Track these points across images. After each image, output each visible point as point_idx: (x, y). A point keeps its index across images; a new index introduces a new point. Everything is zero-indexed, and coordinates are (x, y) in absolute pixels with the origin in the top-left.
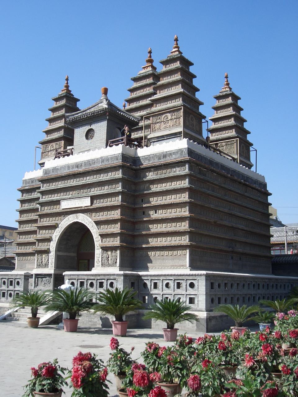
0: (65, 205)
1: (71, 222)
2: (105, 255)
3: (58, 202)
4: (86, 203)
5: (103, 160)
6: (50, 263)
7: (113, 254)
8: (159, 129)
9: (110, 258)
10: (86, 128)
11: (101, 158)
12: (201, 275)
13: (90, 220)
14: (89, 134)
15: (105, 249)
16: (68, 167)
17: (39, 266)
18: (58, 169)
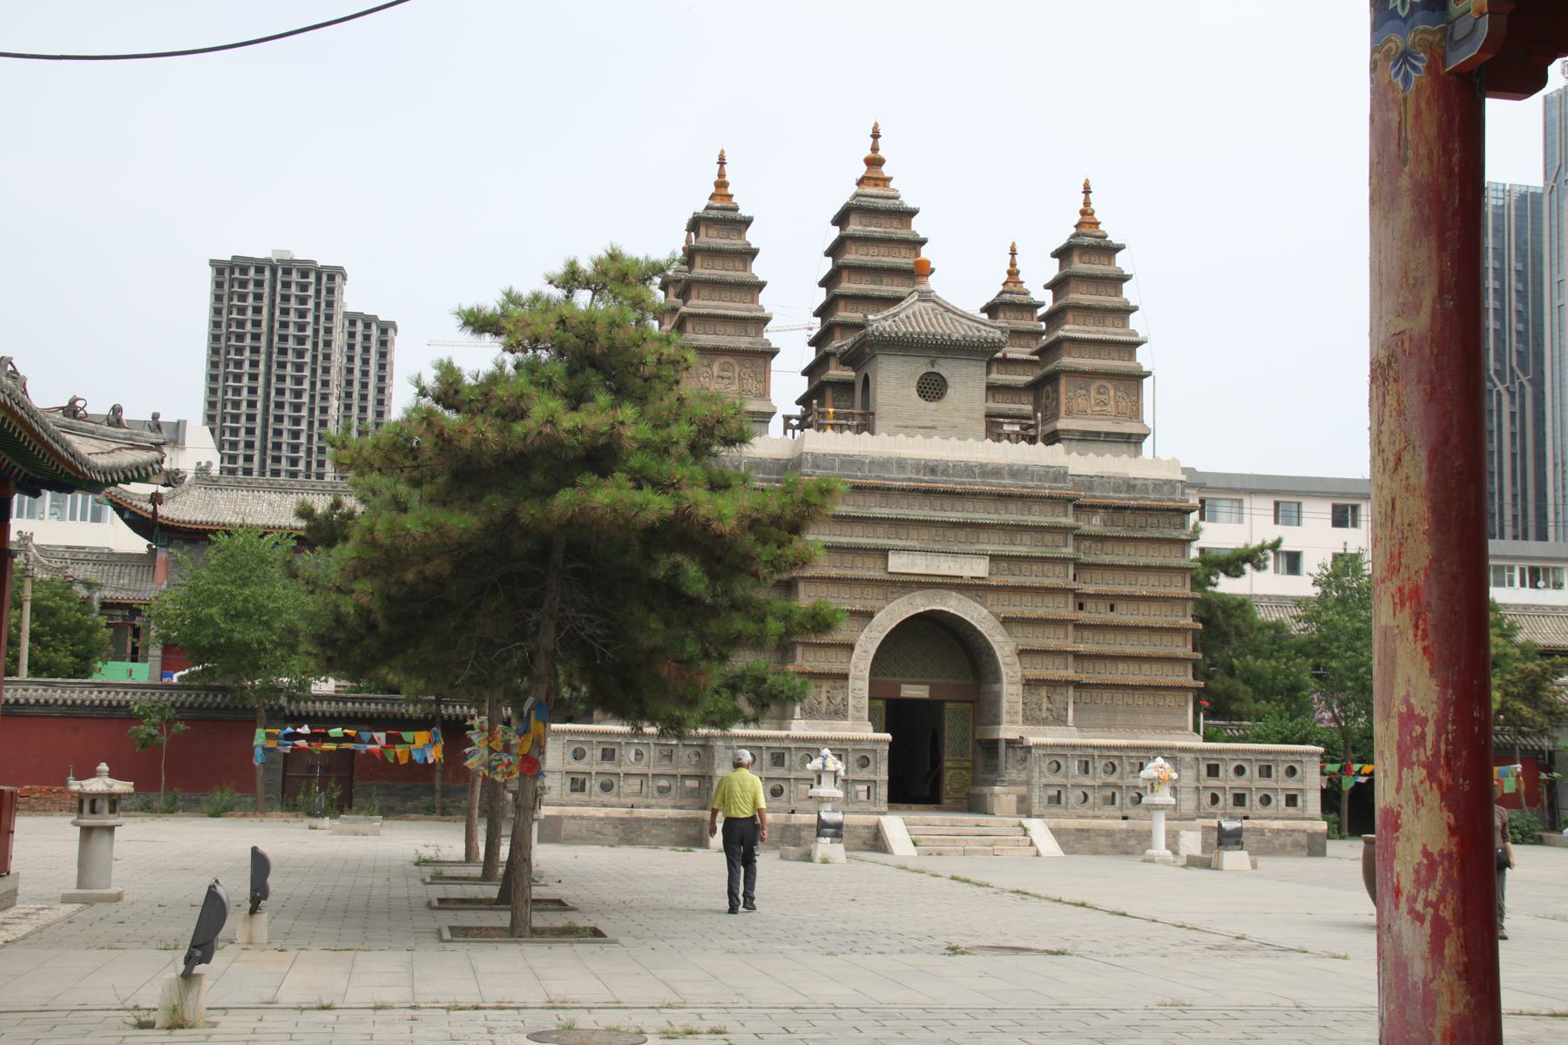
0: (898, 564)
1: (921, 610)
2: (1035, 698)
3: (883, 553)
4: (977, 568)
5: (1015, 472)
6: (851, 709)
7: (1057, 698)
8: (1083, 413)
9: (1044, 707)
10: (920, 367)
11: (1010, 467)
12: (1312, 754)
13: (985, 611)
14: (932, 388)
15: (1030, 684)
16: (901, 464)
17: (810, 714)
18: (863, 463)
